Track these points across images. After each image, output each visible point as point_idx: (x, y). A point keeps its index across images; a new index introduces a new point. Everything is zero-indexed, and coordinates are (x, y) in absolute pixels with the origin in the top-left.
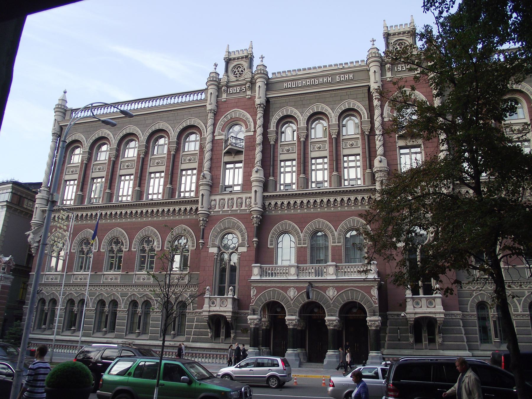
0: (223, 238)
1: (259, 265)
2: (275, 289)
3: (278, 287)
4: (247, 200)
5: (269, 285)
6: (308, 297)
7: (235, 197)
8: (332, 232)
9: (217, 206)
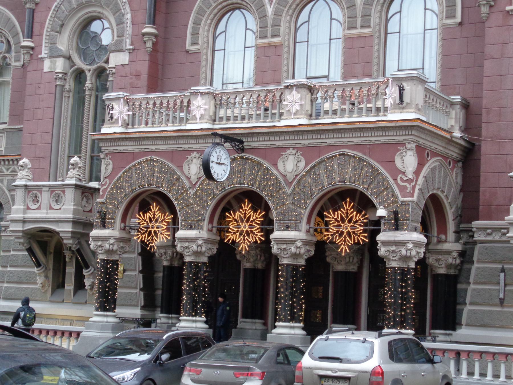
2: (155, 158)
5: (142, 148)
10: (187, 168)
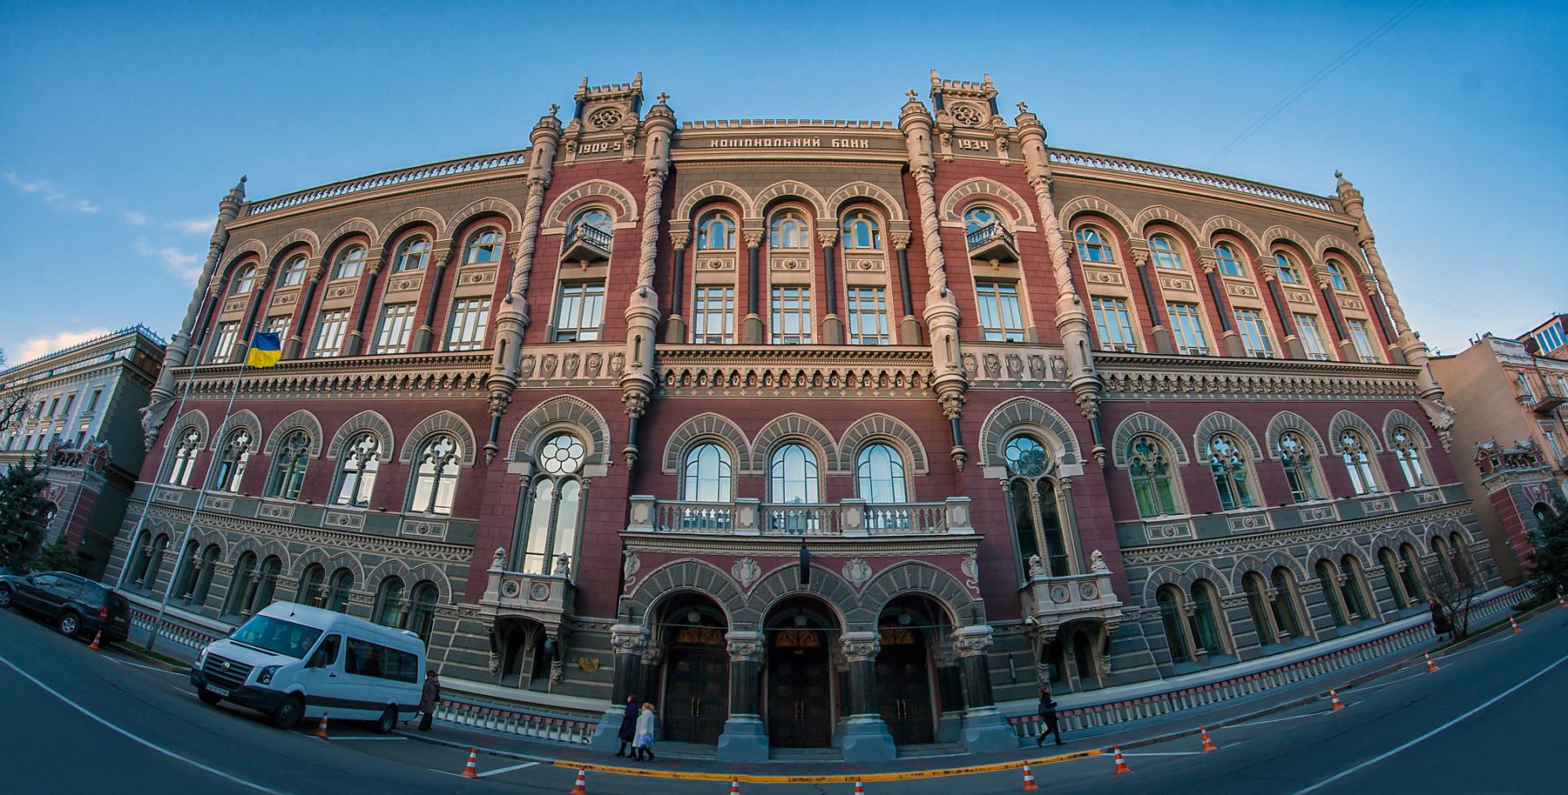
0: (546, 442)
1: (652, 497)
2: (695, 560)
3: (706, 557)
4: (615, 360)
6: (805, 580)
7: (583, 352)
8: (826, 443)
9: (537, 369)
10: (737, 572)
